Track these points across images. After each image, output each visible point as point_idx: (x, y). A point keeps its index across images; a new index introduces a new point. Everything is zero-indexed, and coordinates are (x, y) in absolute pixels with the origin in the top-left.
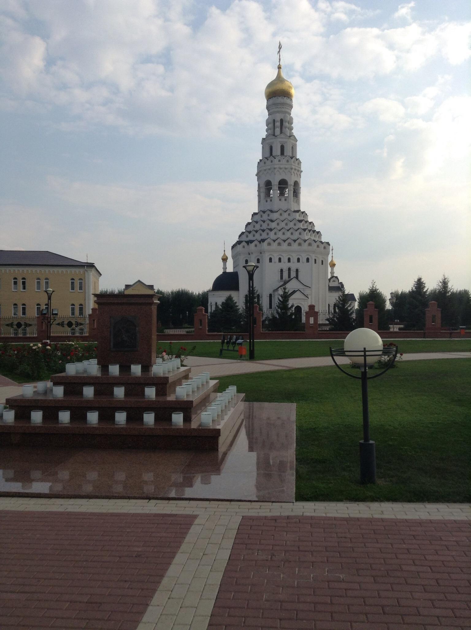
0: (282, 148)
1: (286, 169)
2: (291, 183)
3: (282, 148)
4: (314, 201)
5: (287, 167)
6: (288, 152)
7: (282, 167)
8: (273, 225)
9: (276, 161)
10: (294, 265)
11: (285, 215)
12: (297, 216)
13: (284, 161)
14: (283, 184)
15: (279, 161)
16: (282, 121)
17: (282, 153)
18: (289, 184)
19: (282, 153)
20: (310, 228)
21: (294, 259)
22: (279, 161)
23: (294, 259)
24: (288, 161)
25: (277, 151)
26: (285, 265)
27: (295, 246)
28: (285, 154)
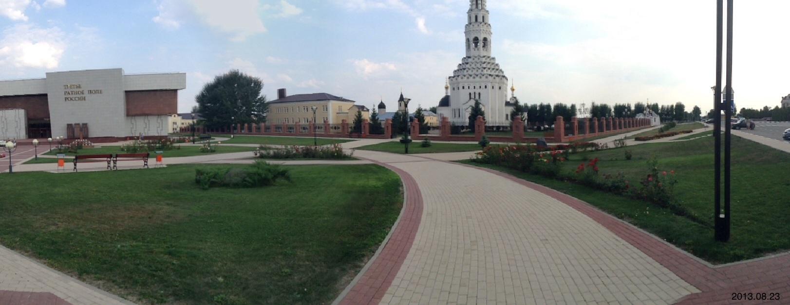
0: (476, 17)
2: (481, 38)
3: (476, 17)
4: (502, 50)
6: (480, 19)
8: (468, 66)
10: (477, 91)
11: (476, 59)
12: (484, 60)
14: (476, 40)
17: (476, 20)
19: (476, 20)
20: (496, 68)
21: (477, 87)
23: (477, 87)
25: (473, 20)
26: (472, 91)
27: (477, 79)
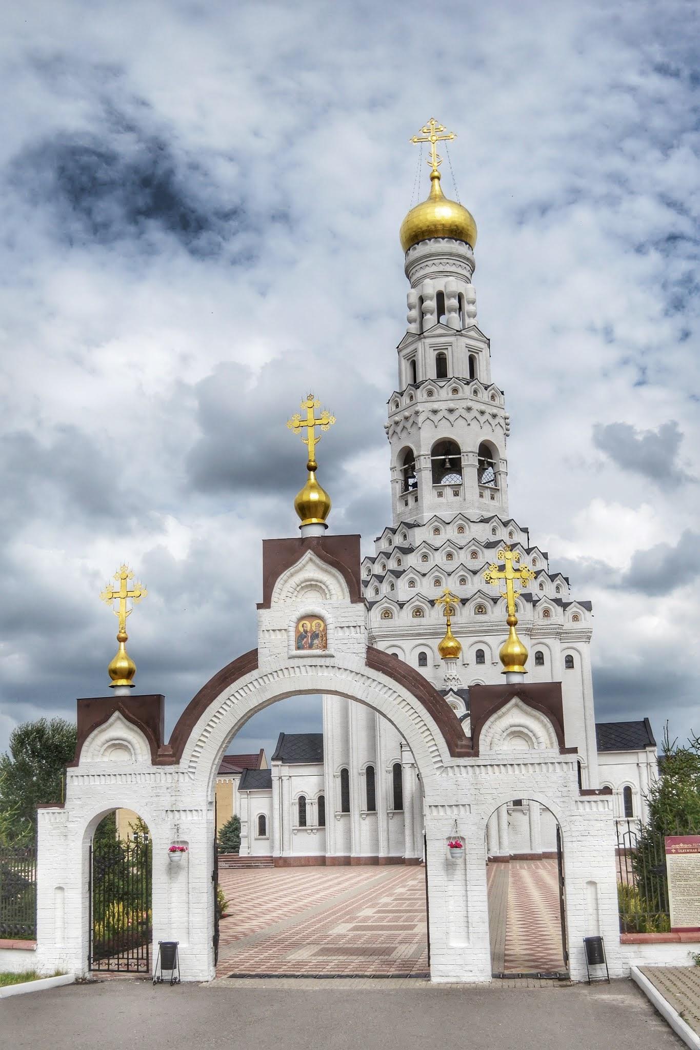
0: (441, 362)
1: (451, 411)
3: (441, 362)
5: (452, 405)
6: (458, 367)
7: (436, 406)
8: (412, 560)
9: (421, 394)
11: (450, 533)
12: (482, 533)
13: (445, 393)
15: (430, 393)
16: (440, 296)
17: (442, 371)
18: (463, 448)
19: (442, 371)
22: (430, 393)
24: (455, 391)
25: (428, 369)
28: (450, 375)
